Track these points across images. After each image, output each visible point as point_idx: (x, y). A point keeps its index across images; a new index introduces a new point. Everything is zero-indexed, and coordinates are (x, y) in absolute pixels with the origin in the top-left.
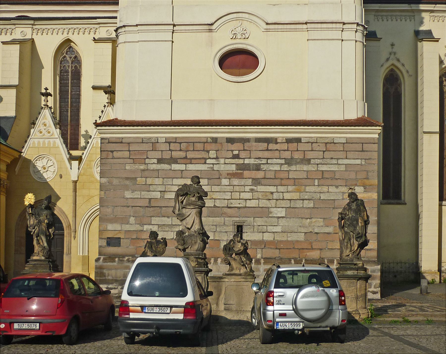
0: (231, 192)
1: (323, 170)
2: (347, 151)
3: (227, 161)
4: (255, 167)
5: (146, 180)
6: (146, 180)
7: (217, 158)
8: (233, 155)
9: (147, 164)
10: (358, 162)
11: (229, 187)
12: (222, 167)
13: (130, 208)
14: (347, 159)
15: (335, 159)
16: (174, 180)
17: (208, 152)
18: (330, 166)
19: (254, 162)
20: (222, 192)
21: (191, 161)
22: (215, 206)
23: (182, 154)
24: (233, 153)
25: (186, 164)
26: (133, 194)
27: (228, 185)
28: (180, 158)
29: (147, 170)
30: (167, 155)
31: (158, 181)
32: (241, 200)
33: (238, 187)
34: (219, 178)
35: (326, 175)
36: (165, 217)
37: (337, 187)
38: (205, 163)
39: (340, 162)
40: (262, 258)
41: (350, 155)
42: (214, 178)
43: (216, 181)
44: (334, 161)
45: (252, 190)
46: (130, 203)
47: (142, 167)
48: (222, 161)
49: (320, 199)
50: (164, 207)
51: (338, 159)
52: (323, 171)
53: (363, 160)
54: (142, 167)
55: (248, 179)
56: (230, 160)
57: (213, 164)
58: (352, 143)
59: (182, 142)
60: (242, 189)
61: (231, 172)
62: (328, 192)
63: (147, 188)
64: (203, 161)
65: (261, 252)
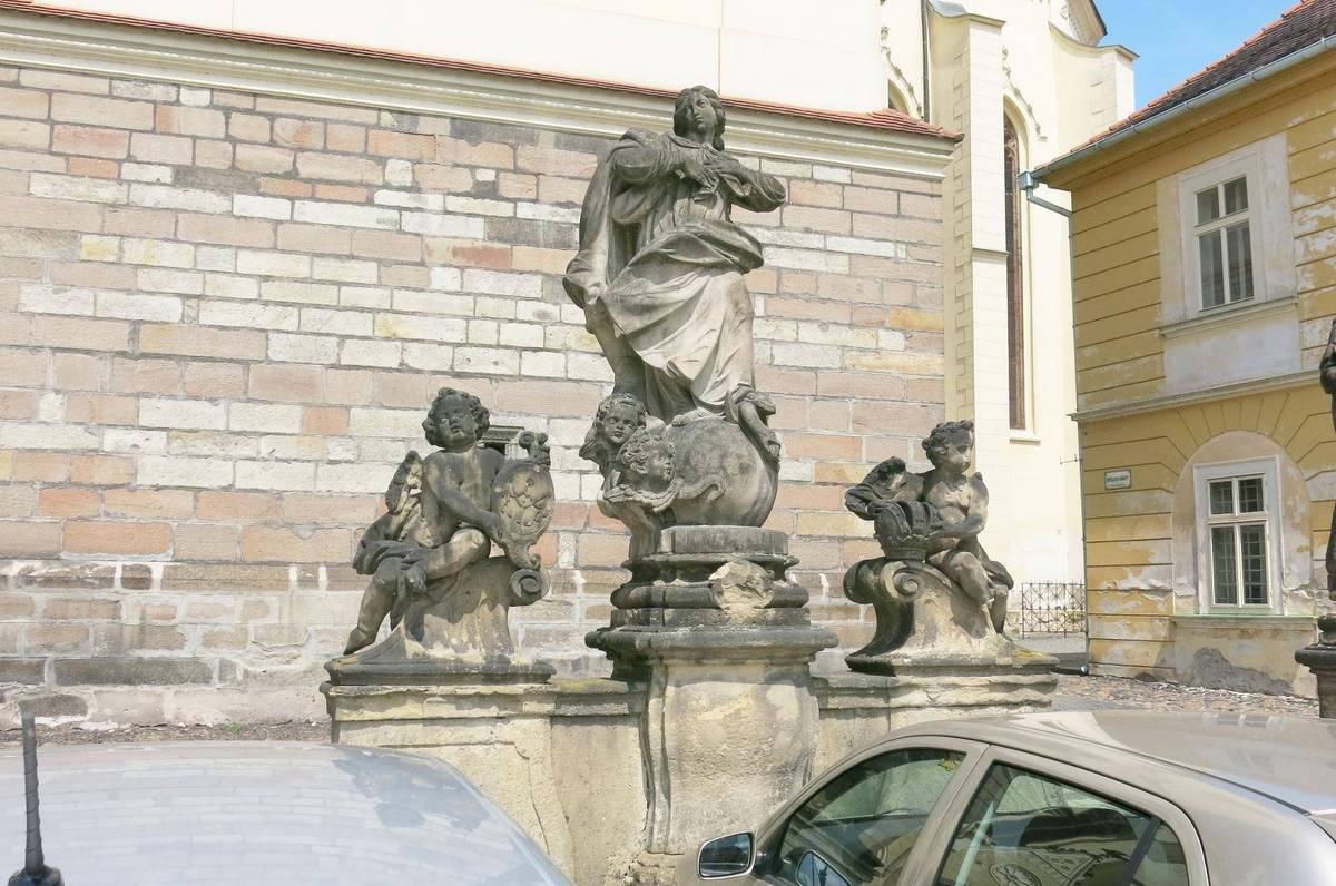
0: (468, 319)
1: (781, 265)
2: (852, 212)
3: (455, 203)
4: (553, 233)
5: (121, 248)
6: (121, 248)
7: (414, 189)
8: (477, 183)
9: (130, 182)
10: (886, 249)
11: (456, 299)
12: (434, 225)
13: (46, 355)
14: (852, 236)
15: (816, 232)
16: (242, 254)
17: (382, 161)
18: (803, 254)
19: (550, 218)
20: (434, 315)
21: (314, 189)
22: (403, 368)
23: (280, 159)
24: (474, 177)
25: (292, 199)
26: (63, 297)
27: (457, 293)
28: (271, 175)
29: (127, 205)
30: (214, 157)
31: (170, 254)
32: (502, 351)
33: (489, 300)
34: (422, 264)
35: (790, 285)
36: (197, 398)
37: (824, 326)
38: (370, 202)
39: (834, 243)
40: (576, 566)
41: (861, 225)
42: (402, 263)
43: (412, 275)
44: (815, 241)
45: (542, 318)
46: (48, 334)
47: (108, 193)
48: (433, 201)
49: (770, 364)
50: (194, 358)
51: (825, 234)
52: (779, 270)
53: (900, 245)
54: (108, 193)
55: (528, 277)
56: (463, 200)
57: (400, 209)
58: (867, 187)
59: (281, 116)
60: (507, 309)
61: (467, 244)
62: (797, 341)
63: (125, 275)
64: (362, 194)
65: (572, 544)
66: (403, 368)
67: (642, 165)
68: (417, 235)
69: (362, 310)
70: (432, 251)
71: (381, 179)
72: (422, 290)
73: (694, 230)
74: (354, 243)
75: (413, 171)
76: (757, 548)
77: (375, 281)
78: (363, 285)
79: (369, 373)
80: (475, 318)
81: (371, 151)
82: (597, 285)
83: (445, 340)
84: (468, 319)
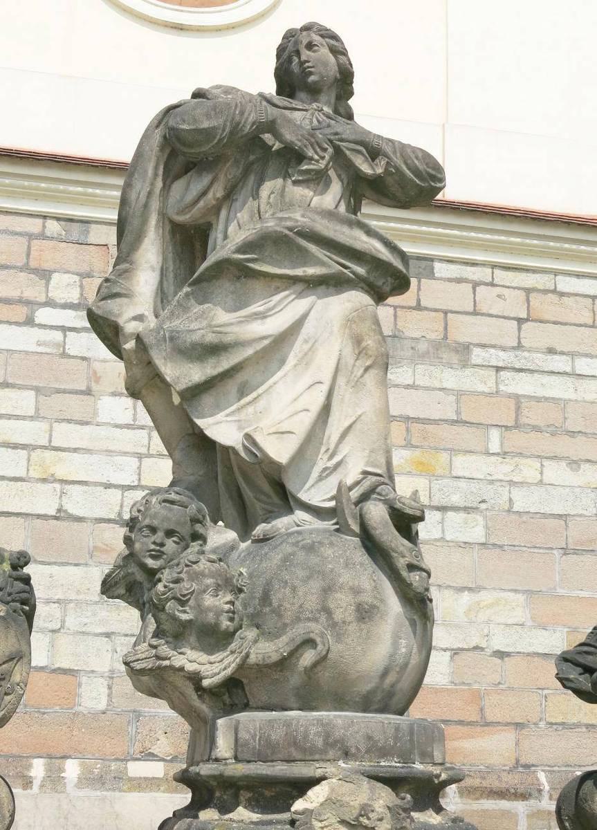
0: (140, 457)
1: (520, 392)
15: (562, 353)
17: (45, 275)
18: (546, 379)
22: (61, 515)
27: (128, 426)
34: (88, 392)
35: (532, 415)
38: (29, 322)
42: (64, 392)
43: (75, 406)
44: (561, 363)
49: (509, 511)
52: (517, 398)
57: (64, 329)
64: (20, 312)
66: (61, 515)
67: (205, 124)
68: (84, 359)
69: (15, 446)
70: (100, 377)
71: (44, 295)
72: (87, 423)
73: (289, 224)
74: (9, 369)
75: (81, 286)
76: (384, 753)
77: (31, 412)
78: (18, 417)
79: (21, 520)
80: (149, 456)
81: (33, 264)
82: (140, 318)
83: (113, 482)
84: (140, 457)
